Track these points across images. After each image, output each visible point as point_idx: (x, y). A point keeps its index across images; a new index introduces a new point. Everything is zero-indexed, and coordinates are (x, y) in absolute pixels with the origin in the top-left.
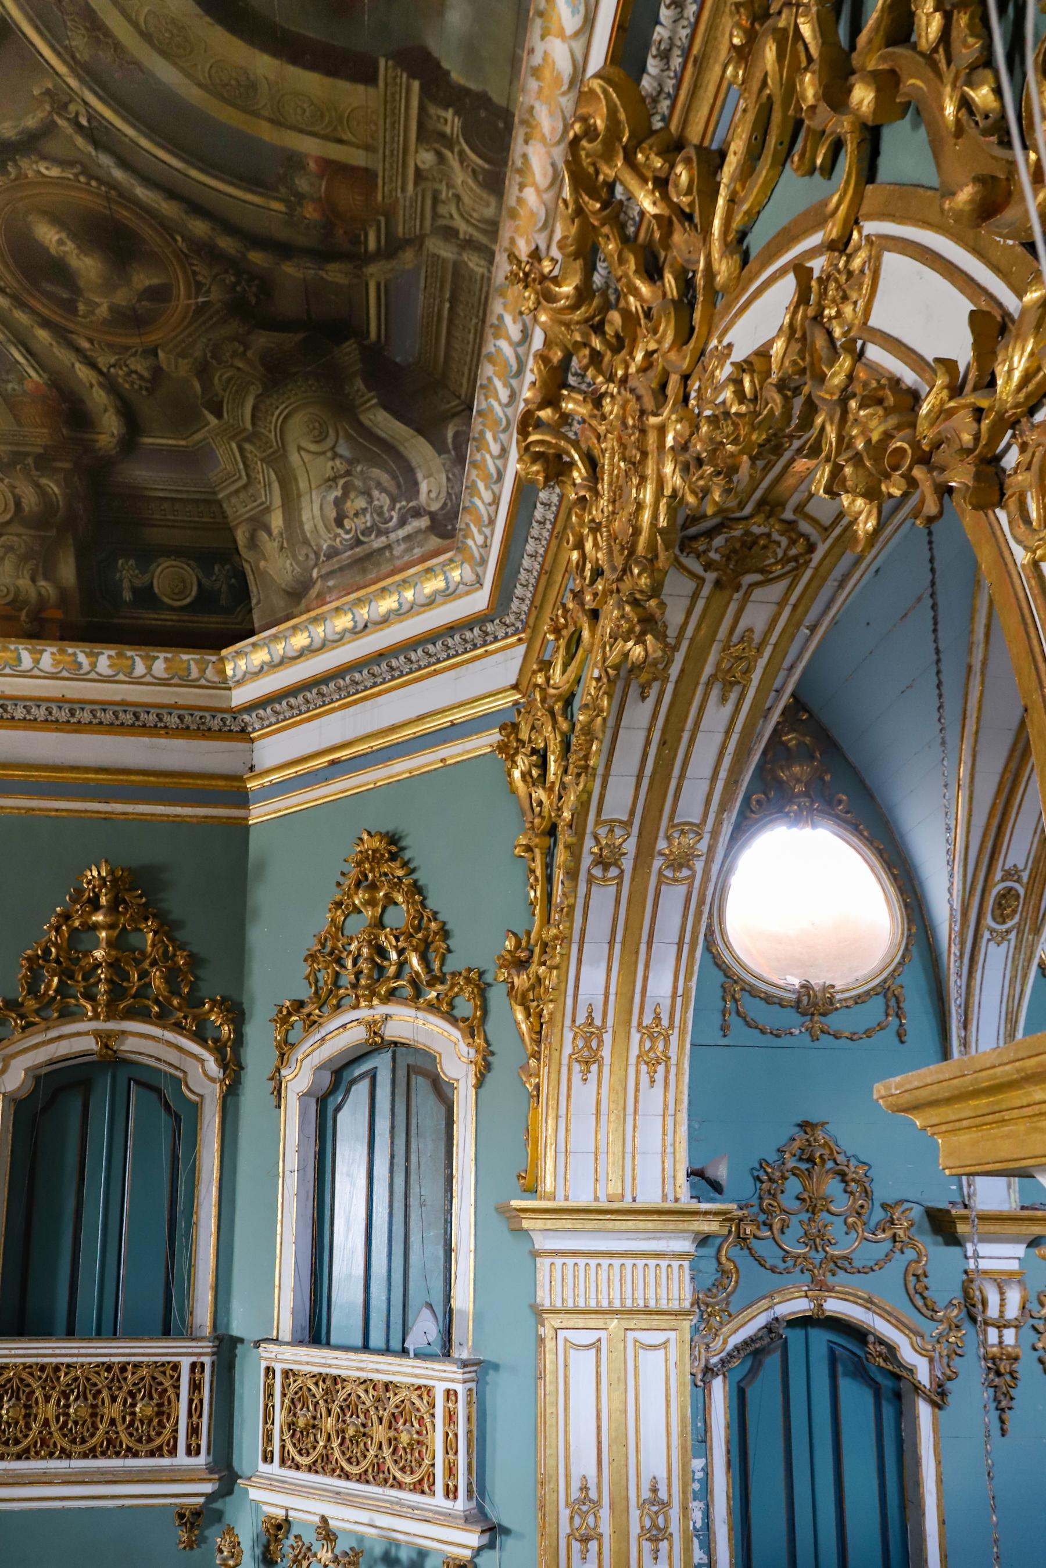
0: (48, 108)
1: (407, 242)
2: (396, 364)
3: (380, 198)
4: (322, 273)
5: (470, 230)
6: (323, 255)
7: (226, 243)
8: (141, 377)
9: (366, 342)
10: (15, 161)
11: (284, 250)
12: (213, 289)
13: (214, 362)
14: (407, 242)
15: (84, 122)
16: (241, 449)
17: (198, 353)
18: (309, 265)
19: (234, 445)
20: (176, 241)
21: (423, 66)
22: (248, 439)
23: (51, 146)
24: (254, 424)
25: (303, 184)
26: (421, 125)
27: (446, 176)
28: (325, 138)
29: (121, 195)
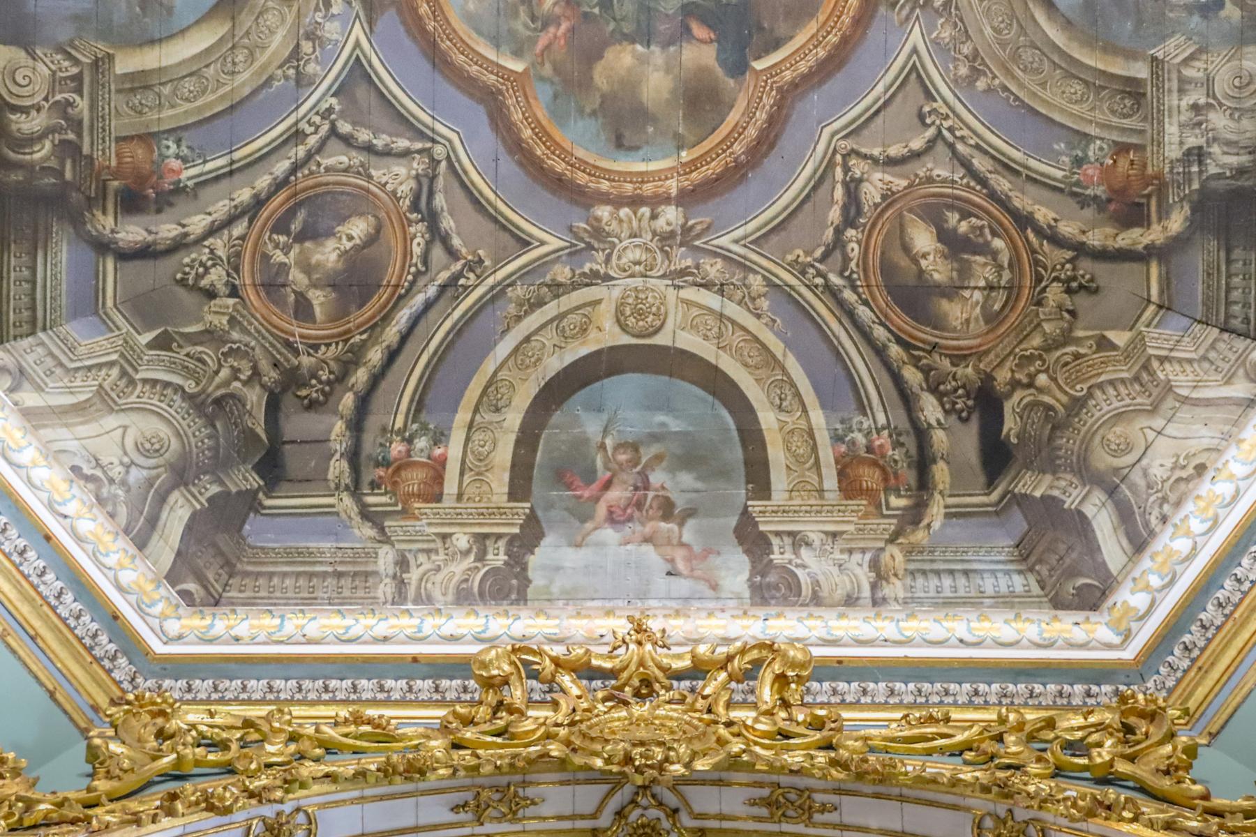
0: (470, 257)
1: (382, 530)
2: (244, 522)
3: (416, 505)
4: (337, 456)
5: (414, 583)
6: (354, 456)
7: (361, 376)
8: (199, 277)
9: (261, 495)
10: (422, 220)
11: (357, 425)
12: (313, 360)
13: (225, 349)
14: (382, 530)
15: (462, 281)
16: (111, 364)
17: (235, 335)
18: (344, 445)
19: (114, 357)
20: (361, 334)
21: (531, 534)
22: (124, 373)
23: (438, 252)
24: (145, 381)
25: (421, 443)
26: (486, 536)
27: (451, 557)
28: (463, 462)
29: (401, 297)
